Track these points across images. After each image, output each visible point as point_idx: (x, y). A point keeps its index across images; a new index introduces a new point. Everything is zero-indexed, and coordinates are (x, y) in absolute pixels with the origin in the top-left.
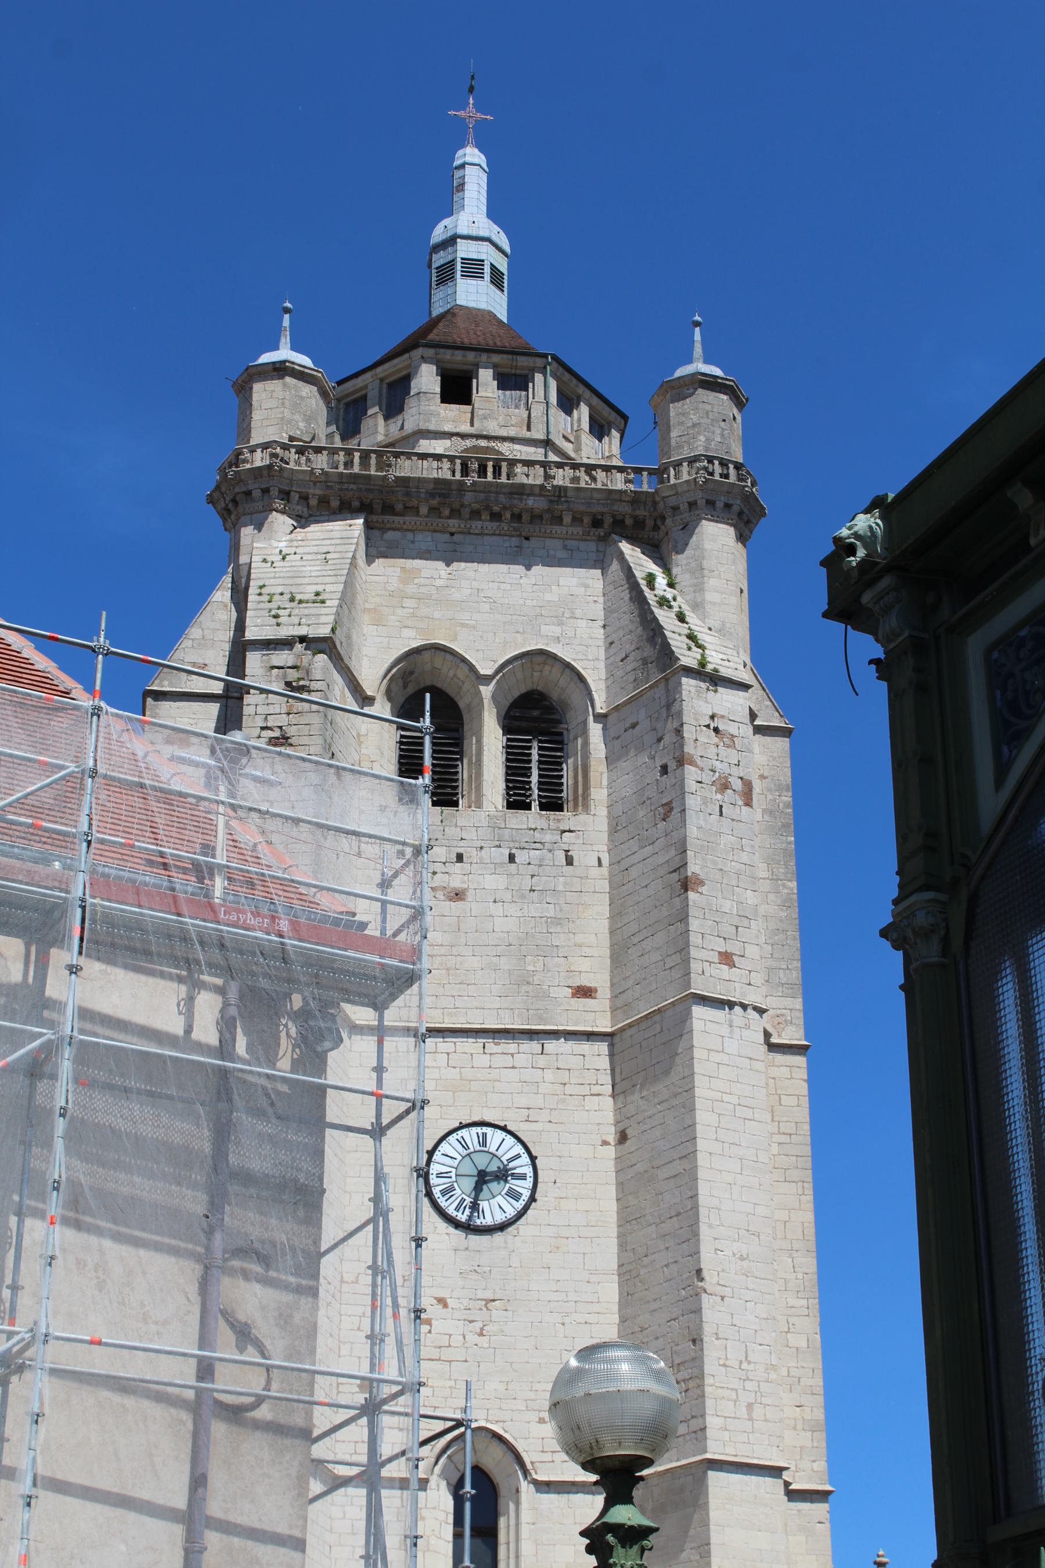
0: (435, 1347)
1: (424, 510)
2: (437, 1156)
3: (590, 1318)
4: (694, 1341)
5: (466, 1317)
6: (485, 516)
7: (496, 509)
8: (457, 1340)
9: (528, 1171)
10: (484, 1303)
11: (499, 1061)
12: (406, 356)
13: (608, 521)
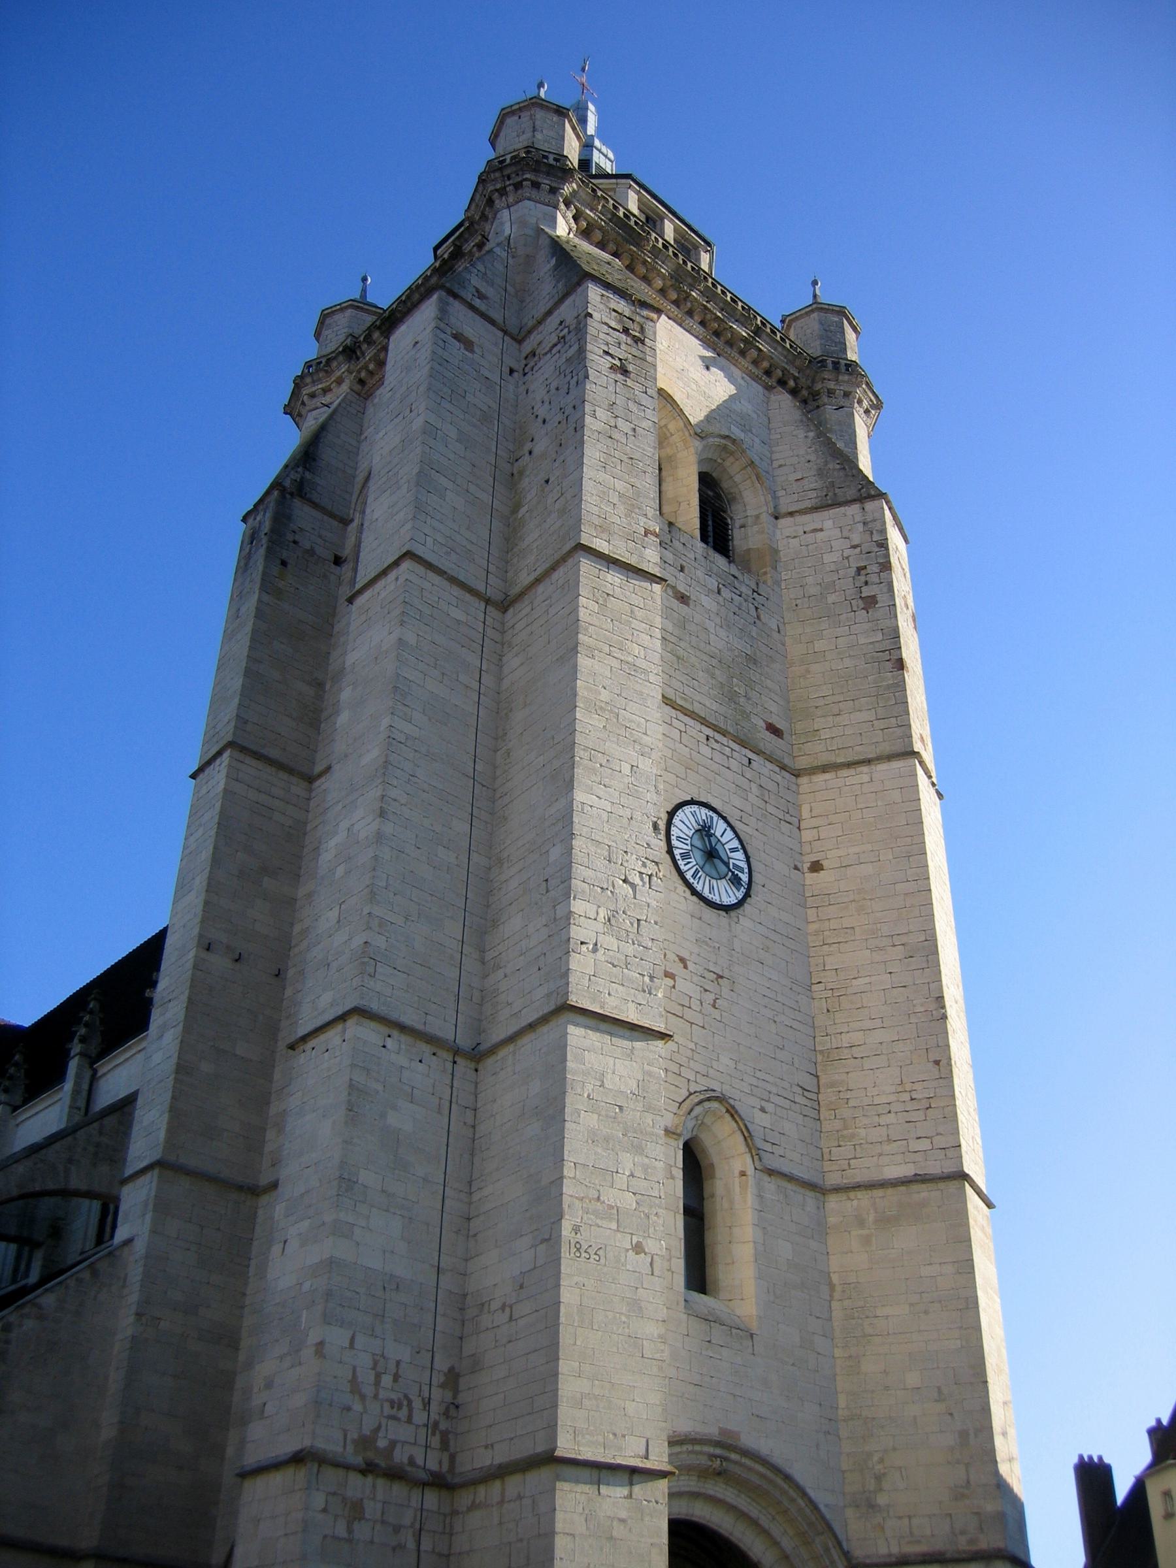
0: (680, 1004)
1: (659, 283)
2: (676, 821)
3: (795, 1025)
4: (937, 1063)
5: (702, 984)
6: (697, 318)
7: (709, 316)
8: (695, 1005)
9: (744, 866)
10: (715, 976)
11: (718, 757)
12: (614, 181)
13: (779, 373)
